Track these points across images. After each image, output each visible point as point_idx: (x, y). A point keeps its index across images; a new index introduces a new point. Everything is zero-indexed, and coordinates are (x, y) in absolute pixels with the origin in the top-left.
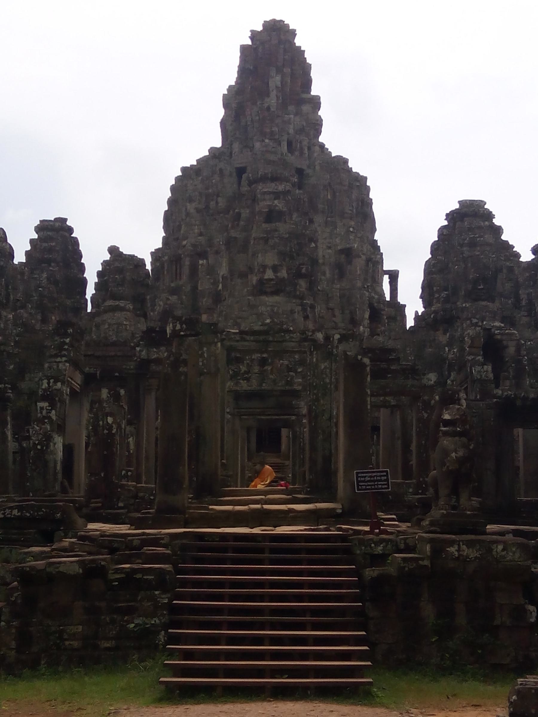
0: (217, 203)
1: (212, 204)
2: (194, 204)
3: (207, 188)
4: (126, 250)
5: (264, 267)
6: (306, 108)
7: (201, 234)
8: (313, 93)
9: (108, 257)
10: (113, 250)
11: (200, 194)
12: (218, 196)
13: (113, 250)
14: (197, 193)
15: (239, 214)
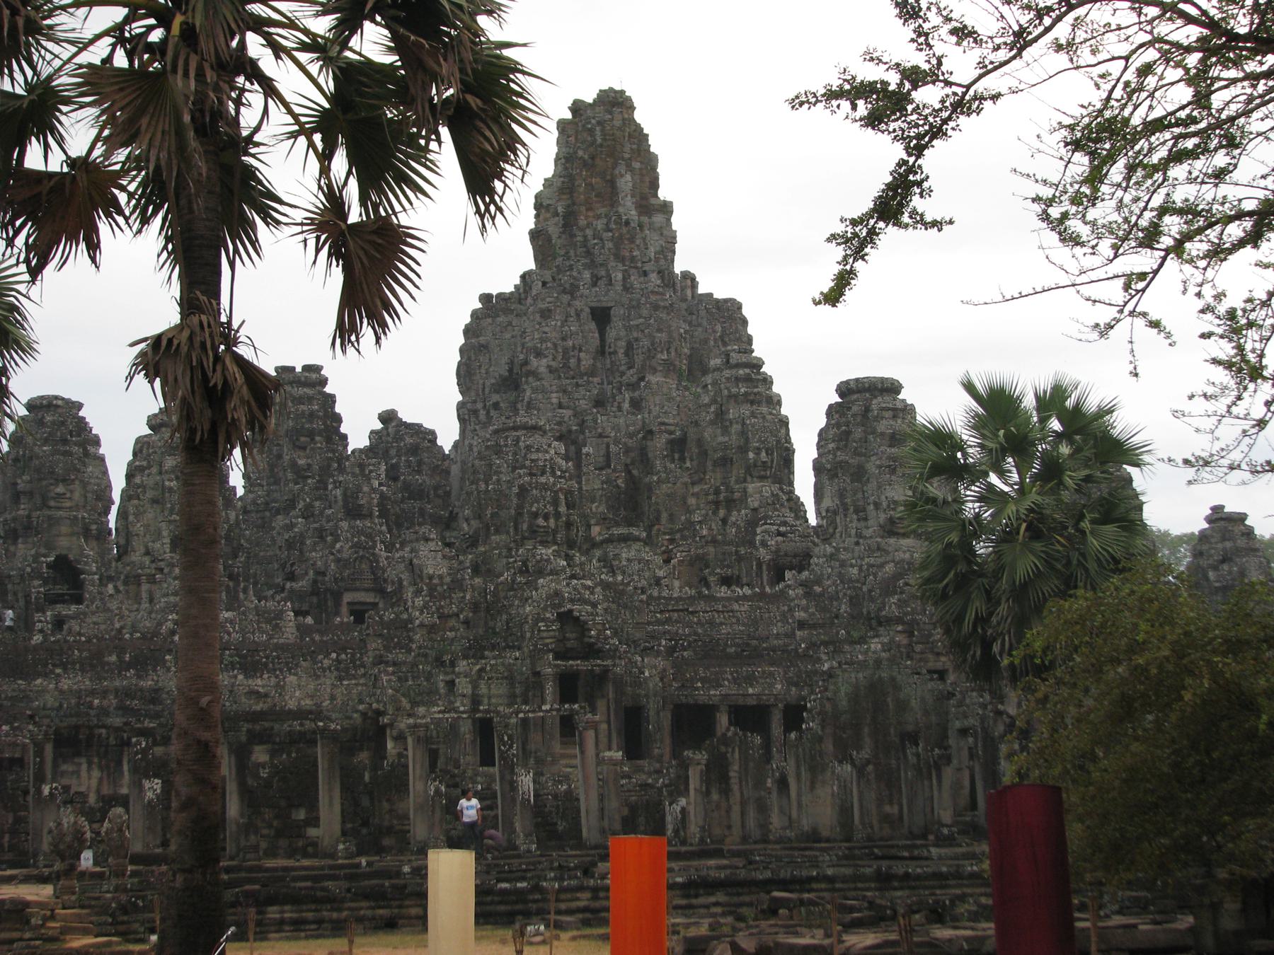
0: (579, 360)
1: (573, 361)
2: (545, 360)
3: (564, 339)
4: (407, 416)
5: (895, 502)
6: (658, 219)
7: (560, 406)
8: (663, 194)
9: (378, 426)
10: (388, 417)
11: (555, 345)
12: (580, 350)
13: (388, 417)
14: (549, 345)
15: (848, 433)
